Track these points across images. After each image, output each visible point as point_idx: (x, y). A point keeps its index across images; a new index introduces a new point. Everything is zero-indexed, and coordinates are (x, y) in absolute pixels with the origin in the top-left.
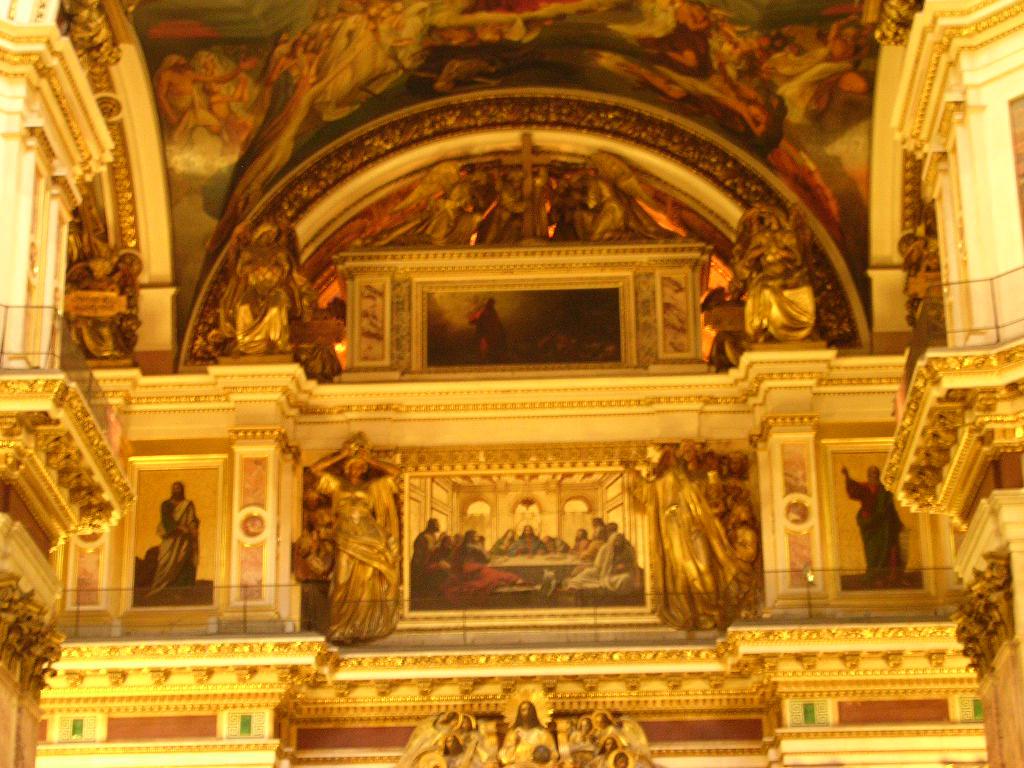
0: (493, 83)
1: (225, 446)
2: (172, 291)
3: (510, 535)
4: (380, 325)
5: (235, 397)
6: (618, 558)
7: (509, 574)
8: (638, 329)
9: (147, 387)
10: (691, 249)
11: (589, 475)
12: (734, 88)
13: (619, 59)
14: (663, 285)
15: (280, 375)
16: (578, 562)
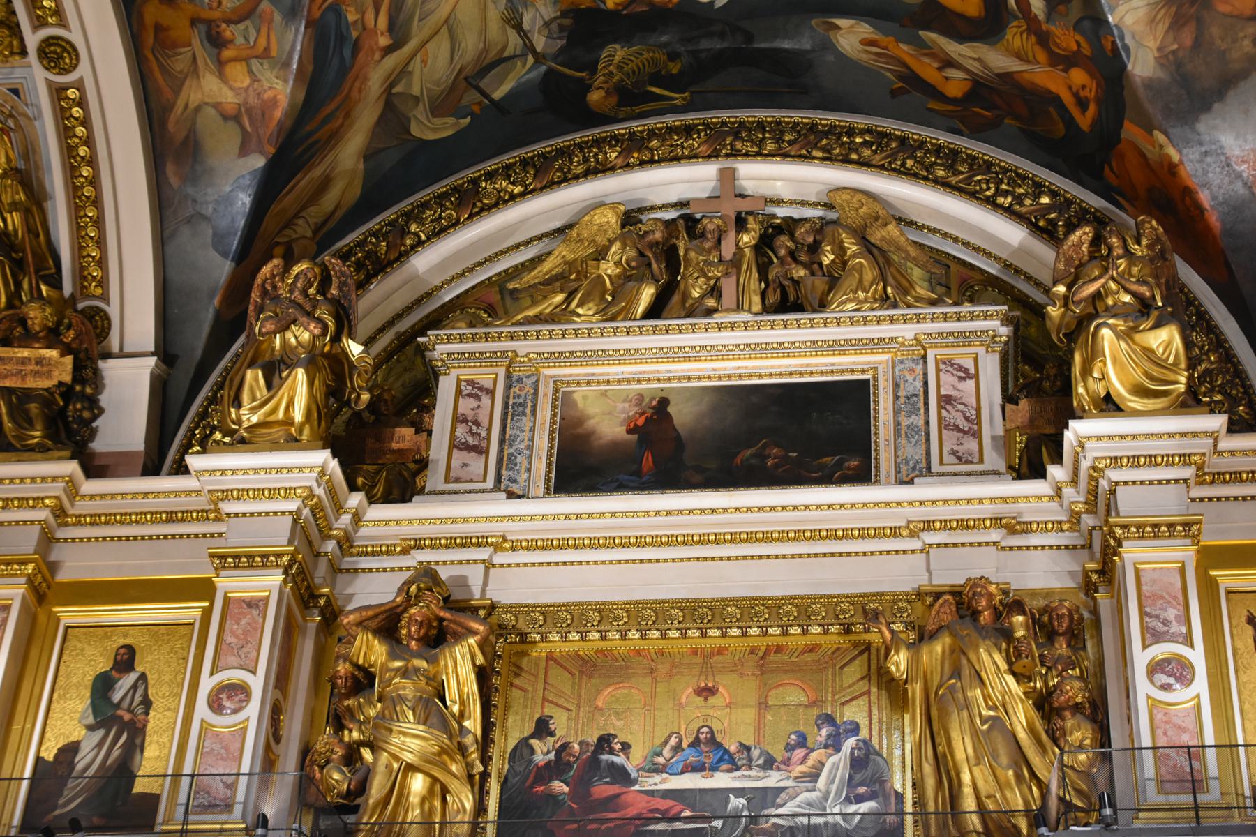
0: (679, 98)
1: (201, 589)
2: (152, 361)
3: (673, 741)
4: (484, 434)
5: (227, 507)
6: (858, 777)
7: (670, 803)
8: (897, 433)
9: (92, 497)
10: (986, 316)
11: (812, 649)
12: (1044, 39)
13: (865, 30)
14: (938, 371)
15: (300, 469)
16: (789, 783)
